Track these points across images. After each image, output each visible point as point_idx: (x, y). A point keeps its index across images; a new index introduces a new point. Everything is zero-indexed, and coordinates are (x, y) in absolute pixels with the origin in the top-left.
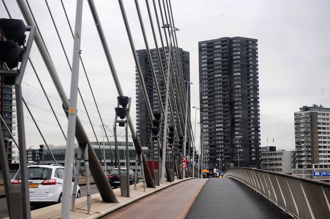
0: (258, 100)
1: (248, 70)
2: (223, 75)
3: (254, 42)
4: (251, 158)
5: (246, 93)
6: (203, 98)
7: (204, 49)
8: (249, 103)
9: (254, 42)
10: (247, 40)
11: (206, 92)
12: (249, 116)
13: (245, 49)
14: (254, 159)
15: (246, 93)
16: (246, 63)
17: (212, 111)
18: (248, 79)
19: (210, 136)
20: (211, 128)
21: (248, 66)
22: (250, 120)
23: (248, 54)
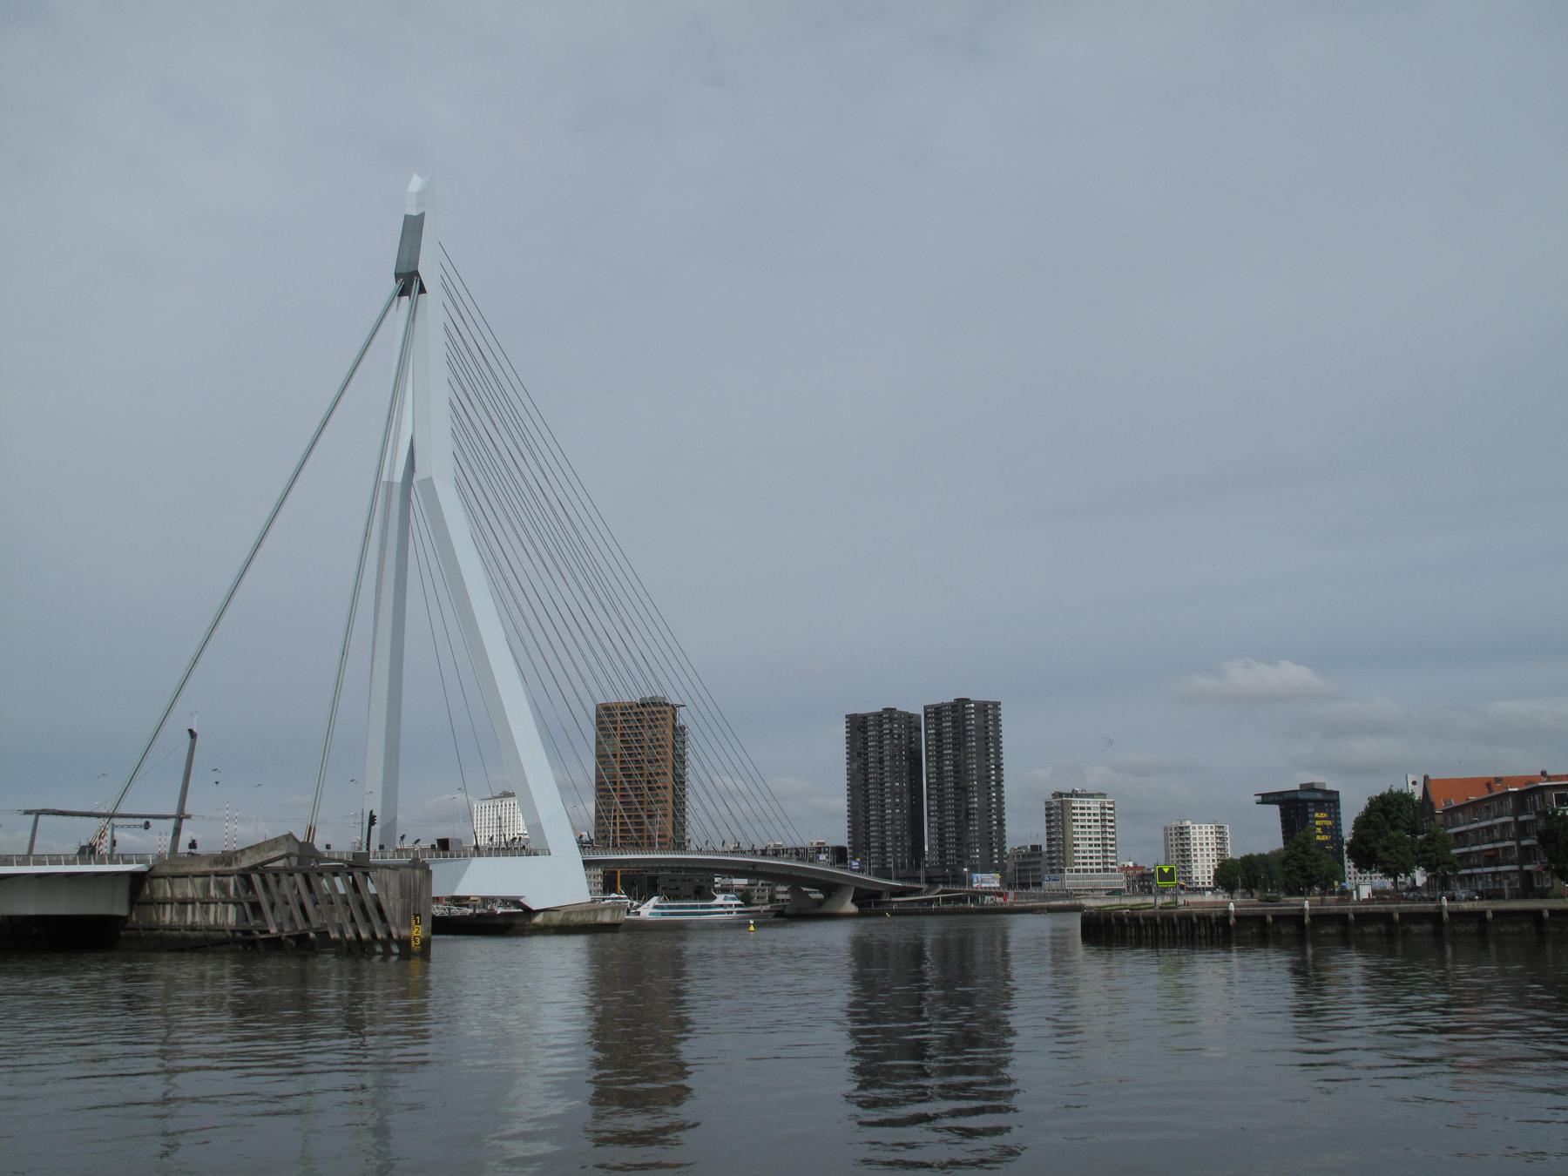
0: (1002, 784)
1: (987, 744)
2: (954, 750)
3: (996, 705)
4: (992, 861)
5: (984, 774)
6: (931, 781)
7: (930, 715)
8: (989, 788)
9: (996, 705)
10: (985, 704)
11: (933, 773)
12: (989, 805)
13: (982, 716)
14: (996, 862)
15: (984, 774)
16: (984, 735)
17: (941, 798)
18: (988, 755)
19: (940, 832)
20: (941, 821)
21: (987, 738)
22: (990, 810)
23: (986, 722)
